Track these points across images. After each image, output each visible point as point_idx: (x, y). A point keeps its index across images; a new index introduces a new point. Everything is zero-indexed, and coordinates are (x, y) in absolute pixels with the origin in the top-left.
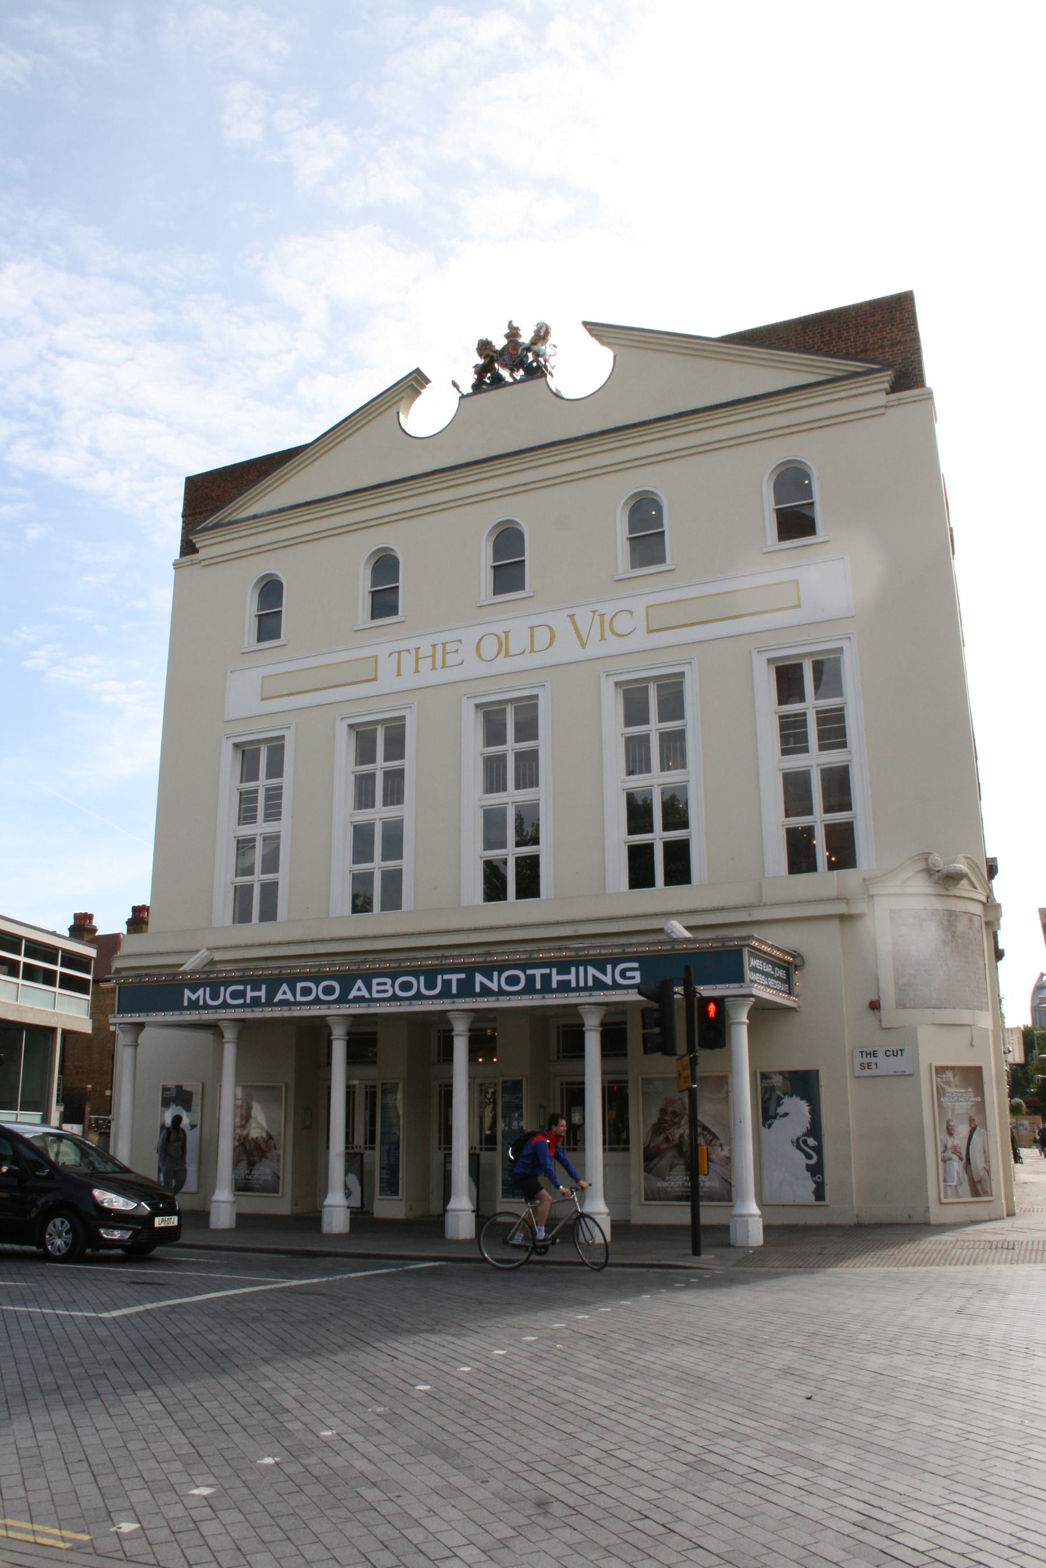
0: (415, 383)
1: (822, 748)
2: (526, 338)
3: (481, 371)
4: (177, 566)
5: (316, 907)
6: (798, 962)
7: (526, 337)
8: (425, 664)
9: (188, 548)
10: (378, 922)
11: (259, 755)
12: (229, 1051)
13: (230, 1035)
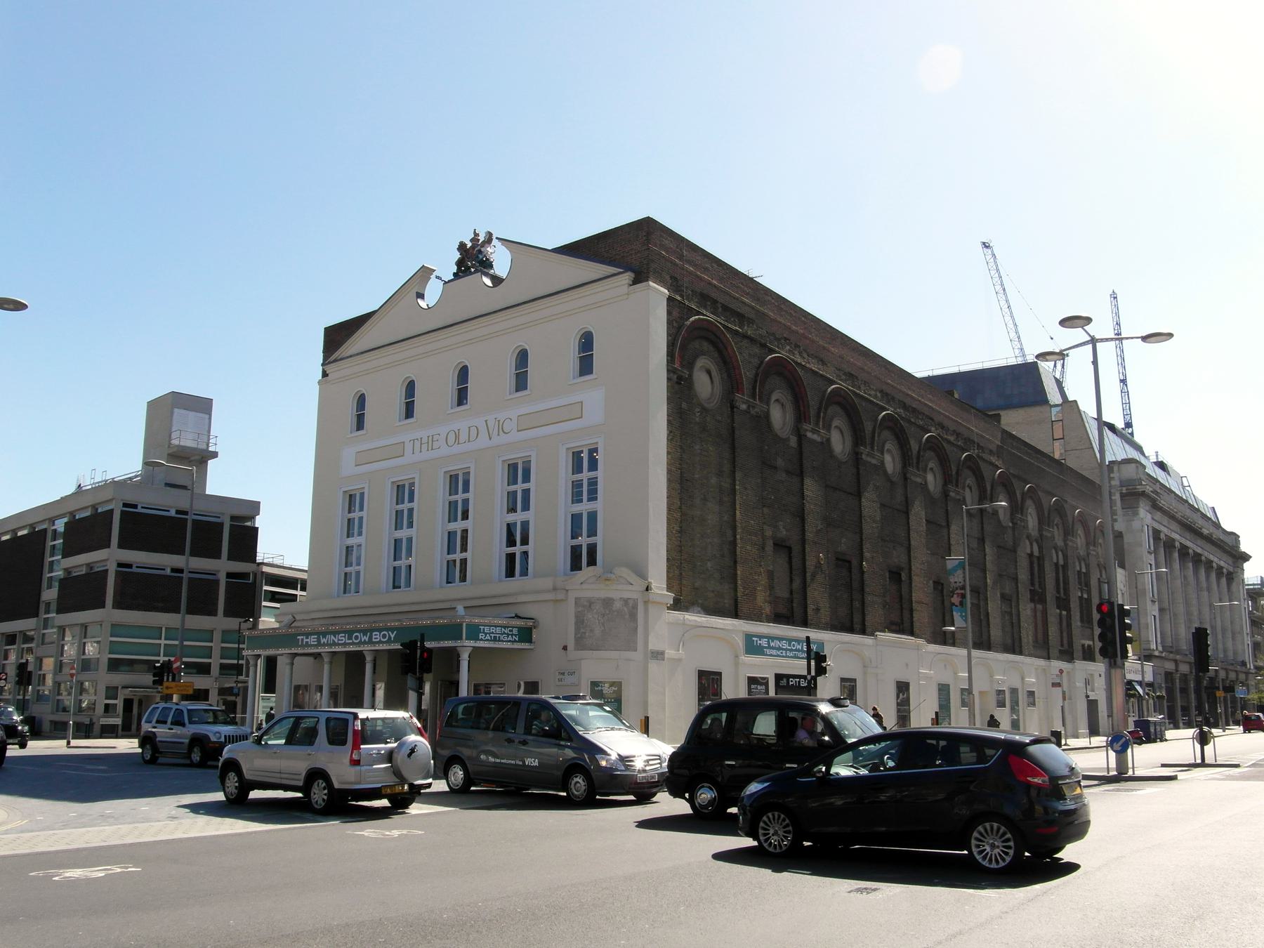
0: (425, 273)
1: (589, 500)
2: (481, 238)
3: (460, 263)
4: (319, 382)
5: (374, 585)
6: (530, 623)
7: (481, 238)
8: (425, 446)
9: (325, 374)
10: (402, 596)
11: (353, 501)
12: (326, 667)
13: (326, 659)
